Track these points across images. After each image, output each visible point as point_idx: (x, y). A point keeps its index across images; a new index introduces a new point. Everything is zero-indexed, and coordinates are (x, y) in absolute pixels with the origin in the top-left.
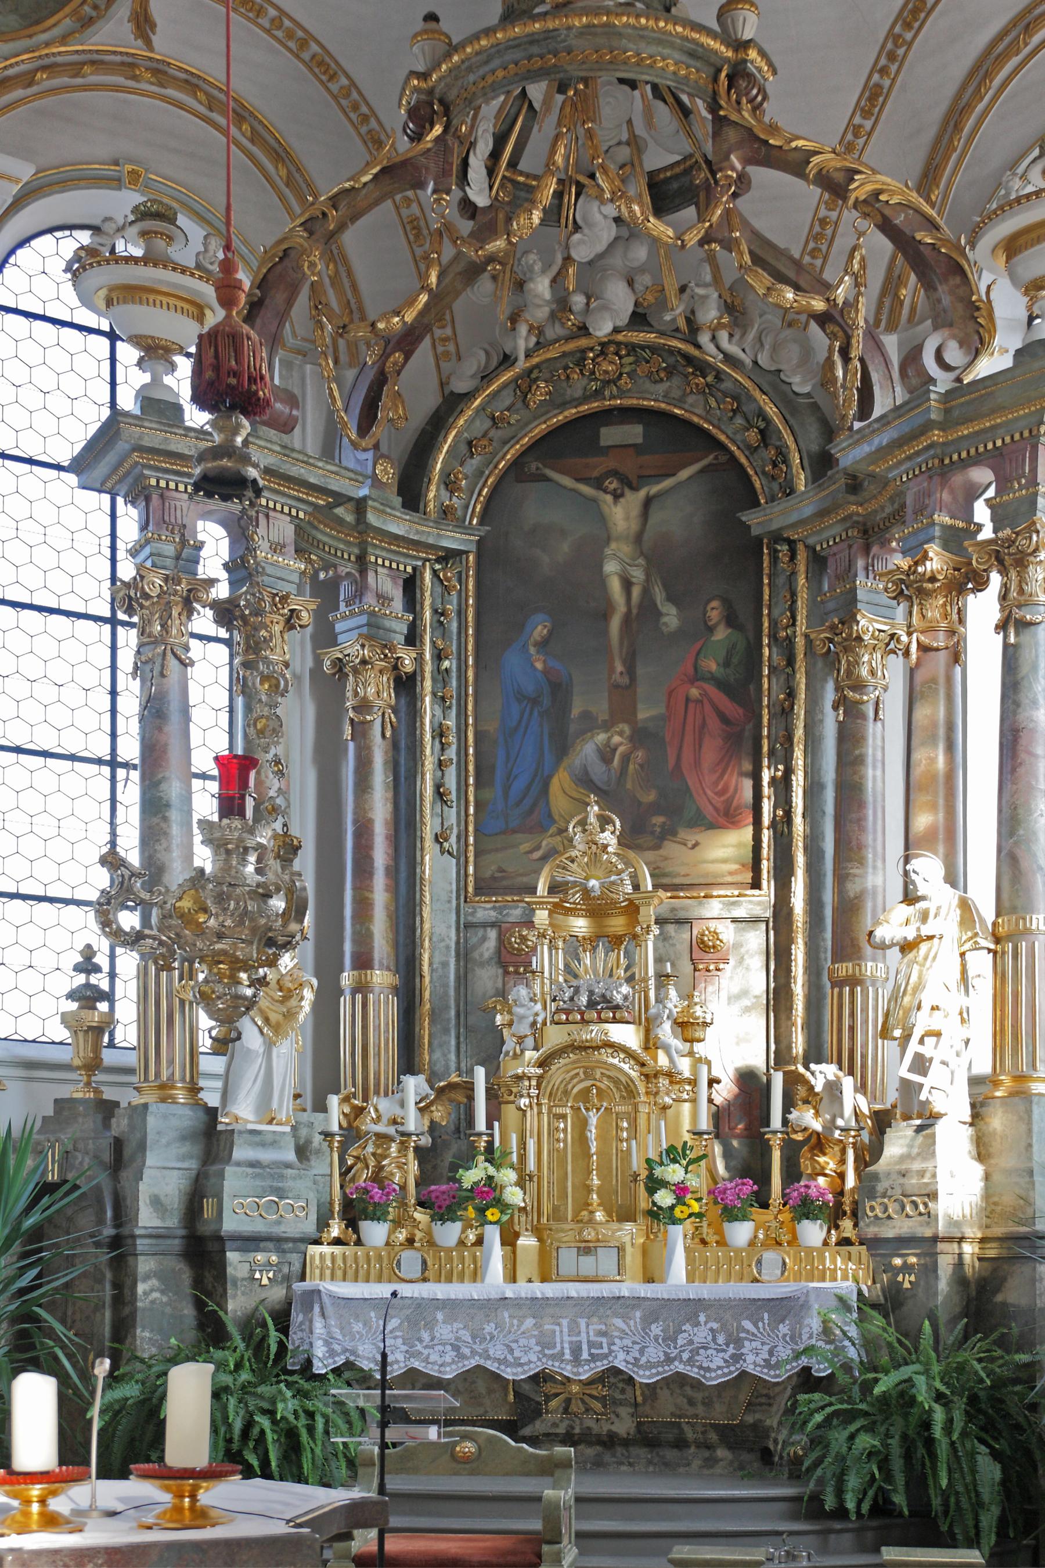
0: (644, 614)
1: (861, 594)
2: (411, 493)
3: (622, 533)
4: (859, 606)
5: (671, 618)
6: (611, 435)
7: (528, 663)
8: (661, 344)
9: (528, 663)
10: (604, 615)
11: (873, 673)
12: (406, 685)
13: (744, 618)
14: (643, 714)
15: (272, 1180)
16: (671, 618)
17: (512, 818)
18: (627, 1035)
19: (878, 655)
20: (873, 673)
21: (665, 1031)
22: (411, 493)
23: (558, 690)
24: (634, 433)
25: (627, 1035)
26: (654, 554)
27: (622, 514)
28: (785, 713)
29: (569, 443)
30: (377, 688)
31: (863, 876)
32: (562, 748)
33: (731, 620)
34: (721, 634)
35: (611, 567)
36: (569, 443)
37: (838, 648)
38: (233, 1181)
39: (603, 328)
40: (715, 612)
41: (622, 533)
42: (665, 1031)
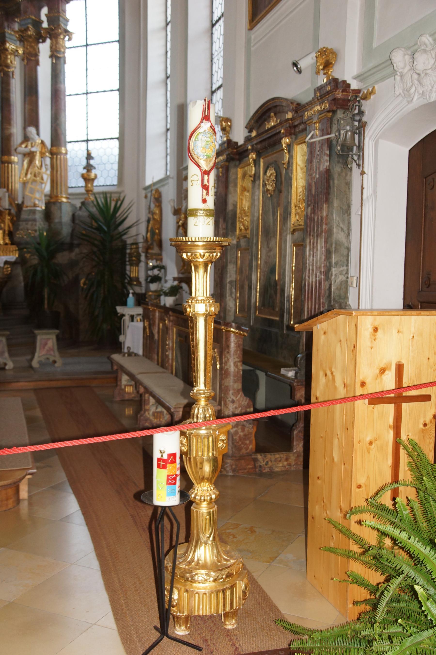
1: (7, 35)
4: (7, 39)
11: (11, 62)
19: (13, 57)
20: (11, 62)
31: (10, 129)
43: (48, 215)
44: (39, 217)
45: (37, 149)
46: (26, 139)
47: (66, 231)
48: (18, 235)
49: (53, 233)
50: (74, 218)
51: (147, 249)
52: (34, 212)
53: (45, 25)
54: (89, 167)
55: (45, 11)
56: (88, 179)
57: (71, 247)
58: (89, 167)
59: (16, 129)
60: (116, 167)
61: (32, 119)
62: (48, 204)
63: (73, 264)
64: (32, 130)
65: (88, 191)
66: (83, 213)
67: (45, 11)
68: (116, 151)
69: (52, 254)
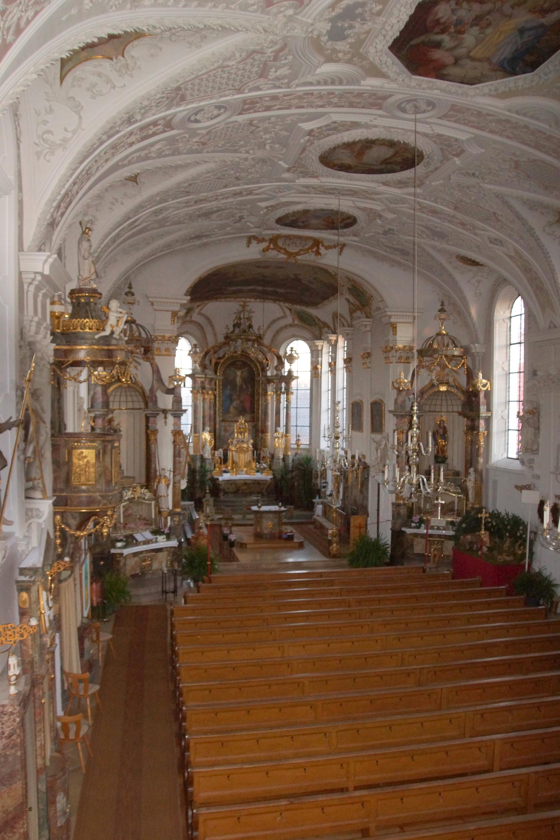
0: (241, 387)
3: (239, 375)
6: (238, 363)
7: (228, 392)
13: (253, 387)
14: (242, 399)
16: (244, 387)
17: (226, 411)
18: (245, 446)
23: (231, 396)
24: (241, 363)
25: (245, 446)
26: (243, 379)
27: (239, 373)
28: (258, 400)
29: (233, 364)
30: (213, 397)
34: (250, 389)
37: (265, 394)
40: (249, 386)
41: (239, 375)
43: (284, 459)
44: (281, 461)
45: (280, 436)
46: (276, 431)
47: (291, 465)
48: (273, 467)
49: (286, 466)
50: (293, 461)
51: (321, 475)
52: (278, 459)
53: (283, 390)
54: (298, 440)
55: (283, 385)
56: (298, 445)
57: (292, 471)
58: (298, 440)
59: (270, 423)
60: (308, 437)
61: (278, 424)
62: (284, 455)
63: (292, 478)
64: (278, 428)
65: (298, 448)
66: (296, 458)
67: (283, 385)
68: (308, 431)
69: (286, 474)
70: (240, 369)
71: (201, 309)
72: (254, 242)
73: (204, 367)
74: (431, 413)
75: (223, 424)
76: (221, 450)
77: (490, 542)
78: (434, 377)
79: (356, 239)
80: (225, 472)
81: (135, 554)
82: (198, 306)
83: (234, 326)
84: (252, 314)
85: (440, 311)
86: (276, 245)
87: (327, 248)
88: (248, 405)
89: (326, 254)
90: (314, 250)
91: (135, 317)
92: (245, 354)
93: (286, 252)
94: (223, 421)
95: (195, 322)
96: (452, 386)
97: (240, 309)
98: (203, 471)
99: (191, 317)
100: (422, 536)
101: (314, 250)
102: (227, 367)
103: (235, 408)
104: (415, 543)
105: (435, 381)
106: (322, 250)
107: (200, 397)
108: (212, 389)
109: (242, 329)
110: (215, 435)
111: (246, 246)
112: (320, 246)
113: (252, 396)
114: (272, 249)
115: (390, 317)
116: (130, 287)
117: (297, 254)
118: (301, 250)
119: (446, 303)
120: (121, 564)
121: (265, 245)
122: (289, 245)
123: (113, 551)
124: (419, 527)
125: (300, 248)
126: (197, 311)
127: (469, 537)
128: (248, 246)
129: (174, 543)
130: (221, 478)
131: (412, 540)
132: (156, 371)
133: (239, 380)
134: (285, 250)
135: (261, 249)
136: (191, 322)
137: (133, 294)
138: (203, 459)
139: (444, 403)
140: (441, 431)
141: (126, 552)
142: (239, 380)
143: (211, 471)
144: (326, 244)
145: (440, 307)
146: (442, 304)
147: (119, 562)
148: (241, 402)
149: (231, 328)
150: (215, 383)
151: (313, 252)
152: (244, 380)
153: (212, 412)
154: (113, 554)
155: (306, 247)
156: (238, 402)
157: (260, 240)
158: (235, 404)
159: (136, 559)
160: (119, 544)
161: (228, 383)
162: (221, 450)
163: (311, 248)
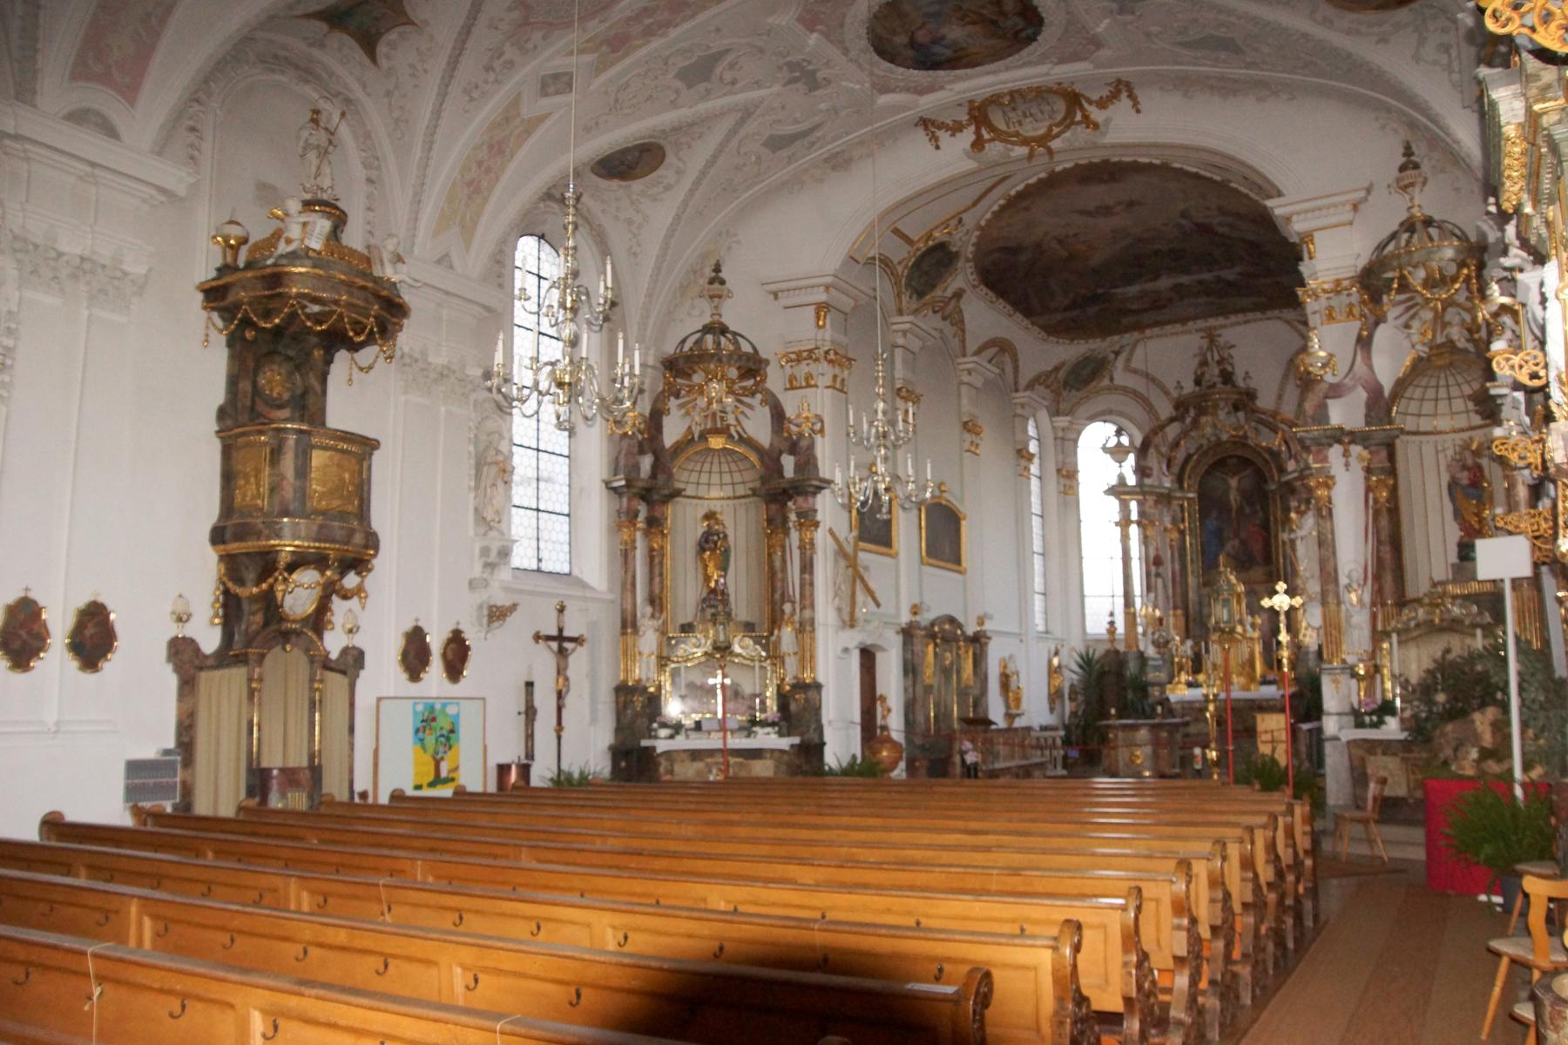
0: (1240, 510)
2: (1181, 487)
5: (1247, 510)
7: (1212, 523)
8: (1241, 442)
9: (1212, 523)
10: (1230, 510)
12: (1182, 533)
13: (1265, 508)
14: (1243, 535)
15: (1157, 668)
16: (1247, 510)
17: (1209, 567)
21: (1248, 628)
22: (1181, 487)
27: (1233, 482)
29: (1220, 464)
30: (1175, 535)
32: (1221, 545)
33: (1262, 508)
34: (1261, 514)
35: (1232, 497)
36: (1220, 464)
38: (1149, 670)
39: (1224, 437)
42: (1248, 628)
44: (1312, 657)
52: (1307, 653)
70: (1234, 474)
71: (1128, 360)
72: (943, 135)
73: (1141, 471)
74: (1438, 438)
75: (1206, 591)
76: (1189, 643)
77: (1494, 733)
78: (1416, 338)
79: (1104, 53)
80: (1190, 685)
81: (695, 755)
82: (1117, 353)
83: (1198, 382)
84: (1232, 352)
85: (1402, 168)
86: (992, 129)
87: (1102, 104)
88: (1257, 548)
89: (1108, 121)
90: (1078, 117)
91: (725, 320)
92: (1241, 442)
93: (1025, 142)
94: (1205, 584)
95: (1125, 390)
96: (1466, 351)
97: (1205, 343)
98: (1142, 688)
99: (1112, 379)
100: (1386, 747)
101: (1078, 117)
102: (1207, 472)
103: (1228, 555)
104: (1369, 771)
105: (1419, 347)
106: (1096, 114)
107: (1134, 530)
108: (1174, 521)
109: (1219, 387)
110: (1187, 616)
111: (930, 148)
112: (1086, 105)
113: (1265, 526)
114: (992, 140)
115: (1288, 219)
116: (717, 269)
117: (1048, 136)
118: (1050, 129)
119: (1420, 151)
120: (662, 770)
121: (968, 135)
122: (1020, 123)
123: (645, 743)
124: (1376, 725)
125: (1047, 123)
126: (1120, 363)
127: (1449, 727)
128: (938, 147)
129: (785, 743)
130: (1173, 698)
131: (1363, 760)
132: (778, 415)
133: (1234, 497)
134: (1017, 134)
135: (967, 146)
136: (1113, 389)
137: (723, 282)
138: (1142, 658)
139: (1442, 393)
140: (1464, 478)
141: (662, 746)
142: (1234, 497)
143: (1162, 685)
144: (1095, 97)
145: (1404, 160)
146: (1408, 152)
147: (657, 765)
148: (1243, 542)
149: (1189, 387)
150: (1182, 506)
151: (1079, 123)
152: (1245, 495)
153: (1177, 567)
154: (647, 748)
155: (1059, 117)
156: (1236, 542)
157: (956, 128)
158: (1229, 546)
159: (699, 765)
160: (663, 733)
161: (1209, 503)
162: (1189, 643)
163: (1070, 114)
